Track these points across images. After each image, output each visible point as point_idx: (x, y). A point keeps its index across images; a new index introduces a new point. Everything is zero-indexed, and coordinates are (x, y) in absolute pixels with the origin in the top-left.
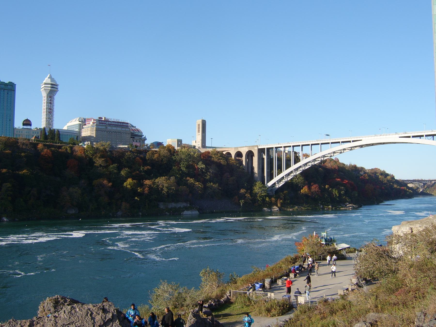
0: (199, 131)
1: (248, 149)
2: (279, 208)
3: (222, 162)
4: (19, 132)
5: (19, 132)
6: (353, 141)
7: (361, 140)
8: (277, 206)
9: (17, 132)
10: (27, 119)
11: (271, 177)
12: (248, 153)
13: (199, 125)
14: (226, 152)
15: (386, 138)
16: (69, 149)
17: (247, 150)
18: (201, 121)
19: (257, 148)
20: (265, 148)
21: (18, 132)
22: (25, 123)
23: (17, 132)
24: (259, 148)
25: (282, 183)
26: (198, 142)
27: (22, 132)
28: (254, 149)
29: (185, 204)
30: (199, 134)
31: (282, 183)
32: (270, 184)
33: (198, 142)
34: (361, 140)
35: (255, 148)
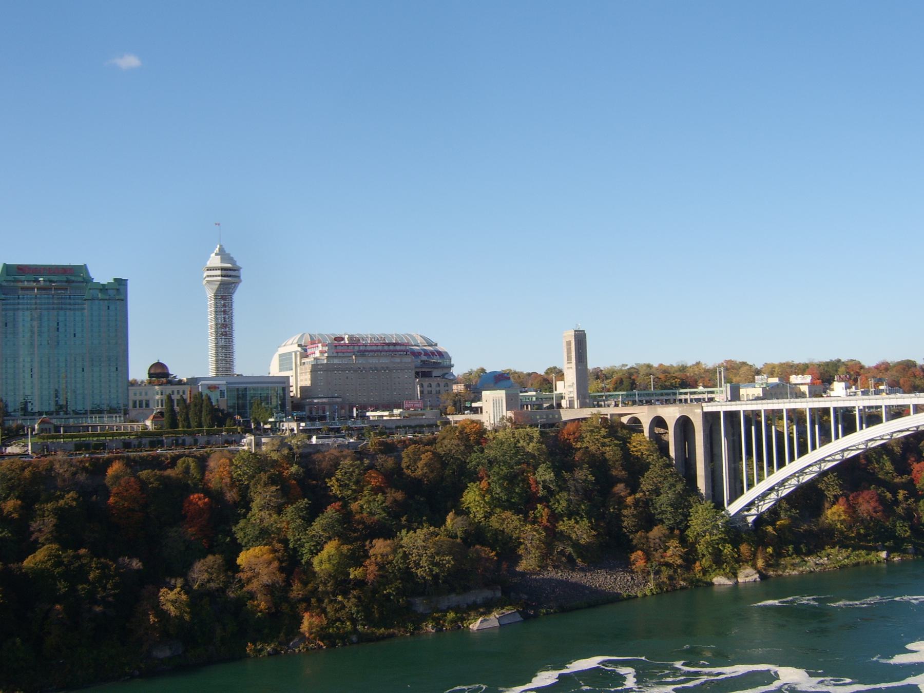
0: (569, 358)
1: (679, 412)
2: (759, 572)
3: (611, 452)
4: (141, 394)
5: (141, 394)
8: (754, 566)
9: (135, 394)
10: (157, 361)
11: (736, 492)
12: (681, 421)
13: (569, 343)
14: (630, 416)
16: (192, 464)
18: (573, 333)
19: (699, 411)
20: (719, 413)
21: (143, 393)
22: (152, 372)
23: (135, 394)
24: (706, 409)
25: (769, 502)
27: (146, 394)
28: (694, 414)
29: (487, 594)
30: (569, 365)
31: (769, 502)
32: (733, 509)
35: (696, 411)
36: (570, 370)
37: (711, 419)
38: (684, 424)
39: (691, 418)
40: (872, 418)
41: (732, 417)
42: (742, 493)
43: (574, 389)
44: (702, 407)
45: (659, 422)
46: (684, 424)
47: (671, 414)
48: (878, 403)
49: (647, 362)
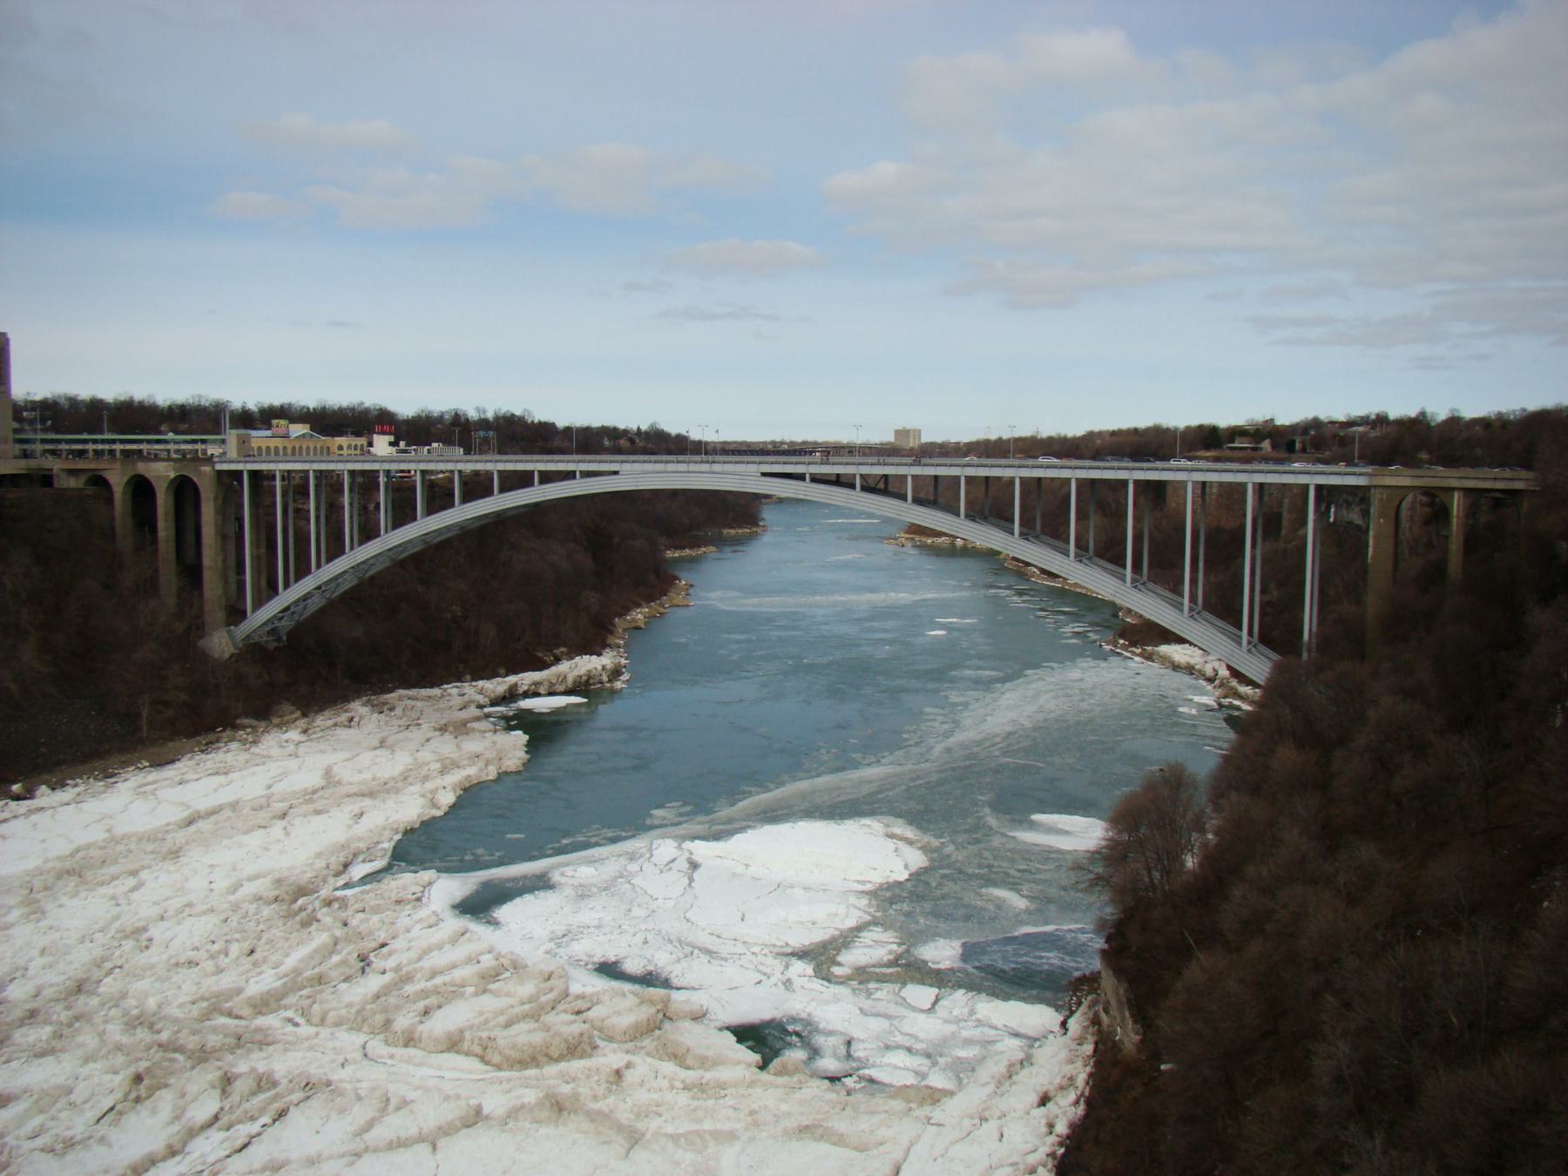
7: (616, 473)
14: (90, 474)
17: (172, 475)
24: (219, 467)
28: (199, 473)
34: (616, 473)
35: (203, 468)
38: (184, 490)
39: (195, 479)
40: (477, 487)
45: (142, 489)
46: (184, 490)
47: (161, 473)
48: (489, 467)
49: (199, 393)
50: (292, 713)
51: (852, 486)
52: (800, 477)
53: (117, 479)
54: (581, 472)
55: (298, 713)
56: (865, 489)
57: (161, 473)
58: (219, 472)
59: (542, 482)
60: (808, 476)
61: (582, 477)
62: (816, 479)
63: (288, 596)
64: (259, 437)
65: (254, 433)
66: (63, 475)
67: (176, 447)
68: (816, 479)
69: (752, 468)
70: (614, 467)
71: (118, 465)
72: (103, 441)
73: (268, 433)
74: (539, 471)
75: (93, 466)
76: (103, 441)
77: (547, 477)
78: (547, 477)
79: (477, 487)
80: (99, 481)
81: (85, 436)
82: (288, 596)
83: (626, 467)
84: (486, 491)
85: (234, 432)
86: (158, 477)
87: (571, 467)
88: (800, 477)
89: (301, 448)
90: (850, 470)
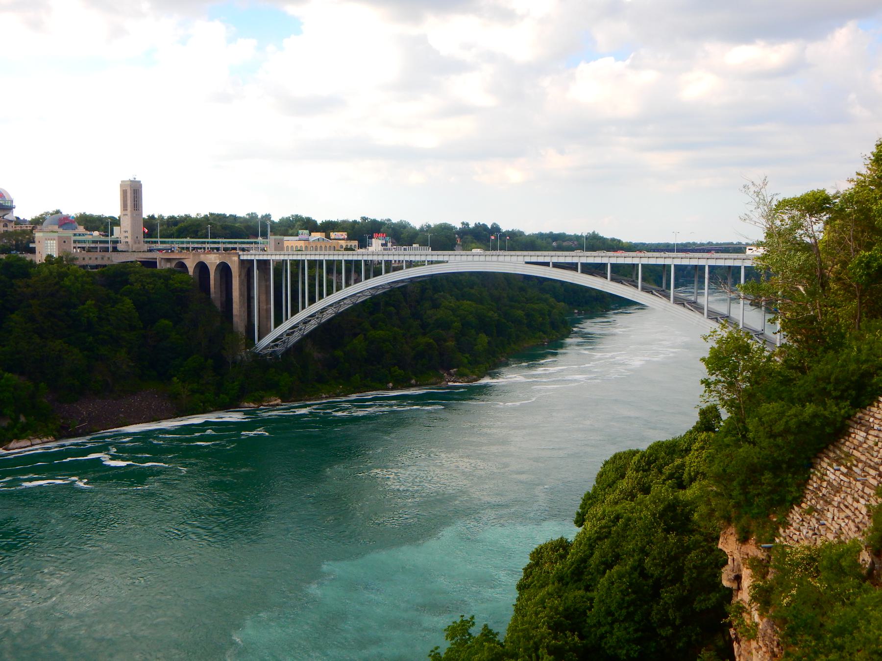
6: (431, 262)
7: (447, 262)
14: (177, 261)
15: (498, 261)
17: (218, 262)
19: (236, 258)
24: (242, 258)
26: (125, 232)
30: (125, 212)
33: (125, 232)
34: (447, 262)
35: (234, 258)
36: (127, 217)
37: (246, 266)
38: (224, 270)
40: (374, 270)
41: (264, 265)
42: (270, 331)
43: (129, 234)
44: (239, 255)
45: (202, 267)
46: (224, 270)
47: (212, 260)
50: (276, 400)
51: (576, 270)
52: (546, 264)
53: (191, 265)
54: (428, 261)
55: (279, 401)
56: (583, 271)
57: (212, 260)
58: (243, 261)
59: (408, 267)
60: (551, 264)
61: (428, 264)
62: (557, 265)
63: (276, 332)
64: (290, 241)
65: (286, 238)
66: (163, 262)
67: (240, 246)
68: (557, 265)
69: (521, 259)
70: (446, 258)
71: (191, 256)
72: (208, 243)
73: (297, 238)
74: (308, 260)
75: (178, 257)
76: (208, 243)
77: (410, 264)
78: (410, 264)
79: (374, 270)
80: (182, 266)
81: (188, 239)
82: (276, 332)
83: (452, 258)
84: (378, 273)
85: (273, 237)
86: (211, 263)
87: (423, 258)
88: (546, 264)
89: (75, 242)
90: (575, 260)
